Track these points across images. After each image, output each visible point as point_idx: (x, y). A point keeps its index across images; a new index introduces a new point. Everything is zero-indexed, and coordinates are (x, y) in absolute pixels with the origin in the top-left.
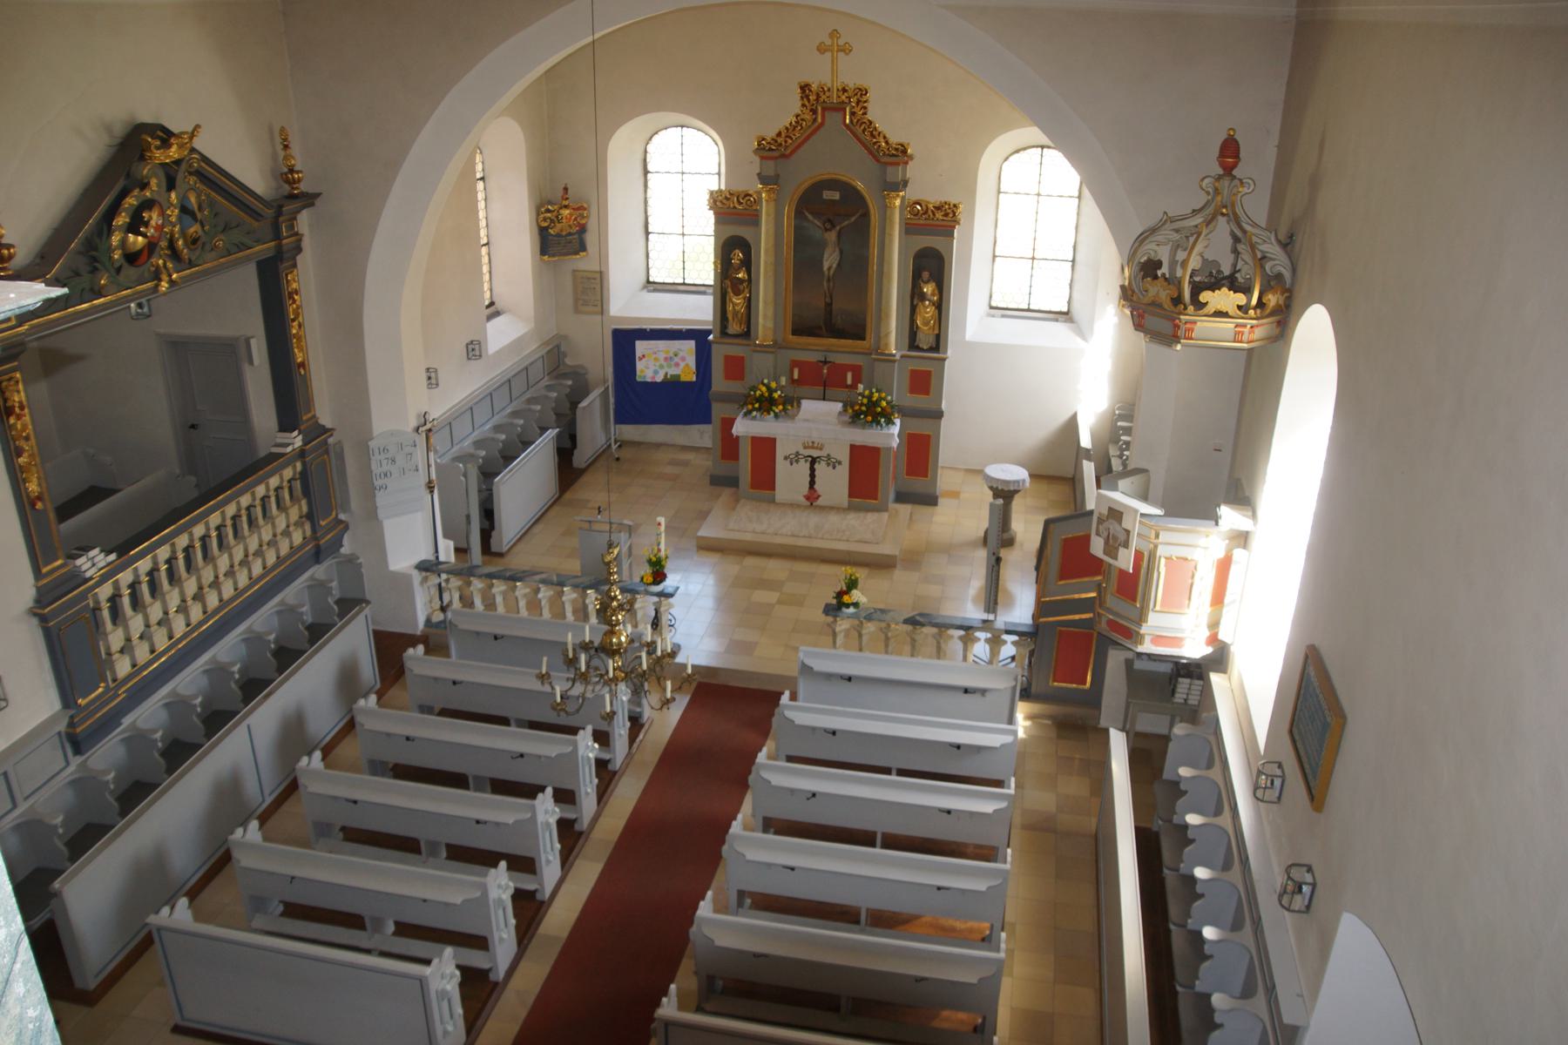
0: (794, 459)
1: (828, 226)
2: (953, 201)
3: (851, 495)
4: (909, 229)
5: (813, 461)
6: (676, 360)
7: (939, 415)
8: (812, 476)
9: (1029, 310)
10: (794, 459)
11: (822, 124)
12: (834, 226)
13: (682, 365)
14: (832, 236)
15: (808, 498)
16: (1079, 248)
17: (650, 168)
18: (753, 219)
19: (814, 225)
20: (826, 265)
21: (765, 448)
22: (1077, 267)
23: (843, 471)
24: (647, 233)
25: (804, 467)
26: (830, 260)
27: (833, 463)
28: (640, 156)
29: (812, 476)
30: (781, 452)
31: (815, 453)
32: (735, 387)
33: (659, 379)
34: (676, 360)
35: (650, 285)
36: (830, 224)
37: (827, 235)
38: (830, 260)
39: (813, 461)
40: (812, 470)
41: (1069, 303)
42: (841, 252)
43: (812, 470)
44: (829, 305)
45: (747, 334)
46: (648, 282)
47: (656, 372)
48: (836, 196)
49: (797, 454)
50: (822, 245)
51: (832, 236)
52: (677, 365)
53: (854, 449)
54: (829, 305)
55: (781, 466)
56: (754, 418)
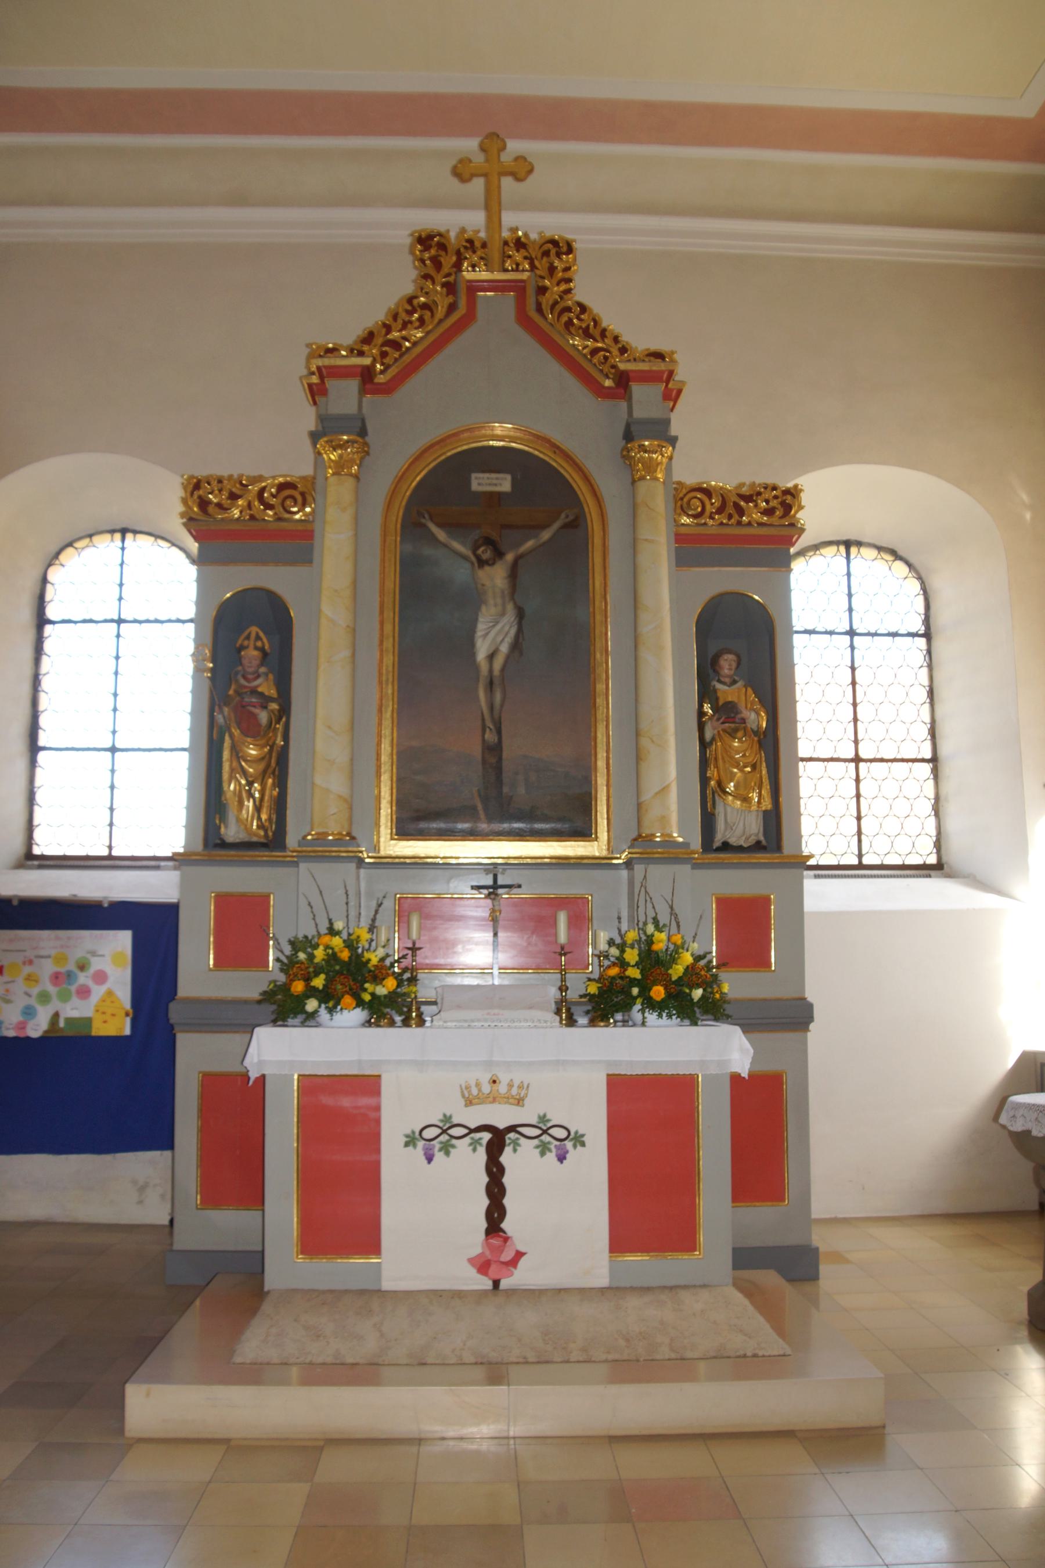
0: (436, 1139)
1: (486, 553)
3: (618, 1244)
4: (689, 550)
5: (498, 1140)
6: (83, 979)
7: (793, 1016)
8: (496, 1190)
9: (860, 868)
10: (436, 1139)
11: (470, 317)
12: (499, 554)
13: (98, 992)
14: (496, 577)
15: (483, 1266)
16: (945, 730)
17: (51, 613)
18: (299, 544)
19: (451, 554)
20: (481, 655)
22: (947, 769)
23: (593, 1162)
24: (34, 748)
25: (469, 1163)
26: (492, 635)
28: (29, 583)
29: (496, 1190)
31: (501, 1117)
33: (37, 1028)
34: (83, 979)
35: (29, 859)
36: (491, 548)
37: (483, 574)
38: (492, 635)
39: (498, 1140)
40: (495, 1171)
41: (938, 845)
42: (521, 614)
43: (495, 1171)
44: (494, 751)
45: (272, 841)
46: (29, 856)
47: (29, 1012)
48: (504, 484)
49: (447, 1126)
50: (471, 601)
51: (496, 577)
52: (84, 992)
54: (494, 751)
56: (310, 1019)
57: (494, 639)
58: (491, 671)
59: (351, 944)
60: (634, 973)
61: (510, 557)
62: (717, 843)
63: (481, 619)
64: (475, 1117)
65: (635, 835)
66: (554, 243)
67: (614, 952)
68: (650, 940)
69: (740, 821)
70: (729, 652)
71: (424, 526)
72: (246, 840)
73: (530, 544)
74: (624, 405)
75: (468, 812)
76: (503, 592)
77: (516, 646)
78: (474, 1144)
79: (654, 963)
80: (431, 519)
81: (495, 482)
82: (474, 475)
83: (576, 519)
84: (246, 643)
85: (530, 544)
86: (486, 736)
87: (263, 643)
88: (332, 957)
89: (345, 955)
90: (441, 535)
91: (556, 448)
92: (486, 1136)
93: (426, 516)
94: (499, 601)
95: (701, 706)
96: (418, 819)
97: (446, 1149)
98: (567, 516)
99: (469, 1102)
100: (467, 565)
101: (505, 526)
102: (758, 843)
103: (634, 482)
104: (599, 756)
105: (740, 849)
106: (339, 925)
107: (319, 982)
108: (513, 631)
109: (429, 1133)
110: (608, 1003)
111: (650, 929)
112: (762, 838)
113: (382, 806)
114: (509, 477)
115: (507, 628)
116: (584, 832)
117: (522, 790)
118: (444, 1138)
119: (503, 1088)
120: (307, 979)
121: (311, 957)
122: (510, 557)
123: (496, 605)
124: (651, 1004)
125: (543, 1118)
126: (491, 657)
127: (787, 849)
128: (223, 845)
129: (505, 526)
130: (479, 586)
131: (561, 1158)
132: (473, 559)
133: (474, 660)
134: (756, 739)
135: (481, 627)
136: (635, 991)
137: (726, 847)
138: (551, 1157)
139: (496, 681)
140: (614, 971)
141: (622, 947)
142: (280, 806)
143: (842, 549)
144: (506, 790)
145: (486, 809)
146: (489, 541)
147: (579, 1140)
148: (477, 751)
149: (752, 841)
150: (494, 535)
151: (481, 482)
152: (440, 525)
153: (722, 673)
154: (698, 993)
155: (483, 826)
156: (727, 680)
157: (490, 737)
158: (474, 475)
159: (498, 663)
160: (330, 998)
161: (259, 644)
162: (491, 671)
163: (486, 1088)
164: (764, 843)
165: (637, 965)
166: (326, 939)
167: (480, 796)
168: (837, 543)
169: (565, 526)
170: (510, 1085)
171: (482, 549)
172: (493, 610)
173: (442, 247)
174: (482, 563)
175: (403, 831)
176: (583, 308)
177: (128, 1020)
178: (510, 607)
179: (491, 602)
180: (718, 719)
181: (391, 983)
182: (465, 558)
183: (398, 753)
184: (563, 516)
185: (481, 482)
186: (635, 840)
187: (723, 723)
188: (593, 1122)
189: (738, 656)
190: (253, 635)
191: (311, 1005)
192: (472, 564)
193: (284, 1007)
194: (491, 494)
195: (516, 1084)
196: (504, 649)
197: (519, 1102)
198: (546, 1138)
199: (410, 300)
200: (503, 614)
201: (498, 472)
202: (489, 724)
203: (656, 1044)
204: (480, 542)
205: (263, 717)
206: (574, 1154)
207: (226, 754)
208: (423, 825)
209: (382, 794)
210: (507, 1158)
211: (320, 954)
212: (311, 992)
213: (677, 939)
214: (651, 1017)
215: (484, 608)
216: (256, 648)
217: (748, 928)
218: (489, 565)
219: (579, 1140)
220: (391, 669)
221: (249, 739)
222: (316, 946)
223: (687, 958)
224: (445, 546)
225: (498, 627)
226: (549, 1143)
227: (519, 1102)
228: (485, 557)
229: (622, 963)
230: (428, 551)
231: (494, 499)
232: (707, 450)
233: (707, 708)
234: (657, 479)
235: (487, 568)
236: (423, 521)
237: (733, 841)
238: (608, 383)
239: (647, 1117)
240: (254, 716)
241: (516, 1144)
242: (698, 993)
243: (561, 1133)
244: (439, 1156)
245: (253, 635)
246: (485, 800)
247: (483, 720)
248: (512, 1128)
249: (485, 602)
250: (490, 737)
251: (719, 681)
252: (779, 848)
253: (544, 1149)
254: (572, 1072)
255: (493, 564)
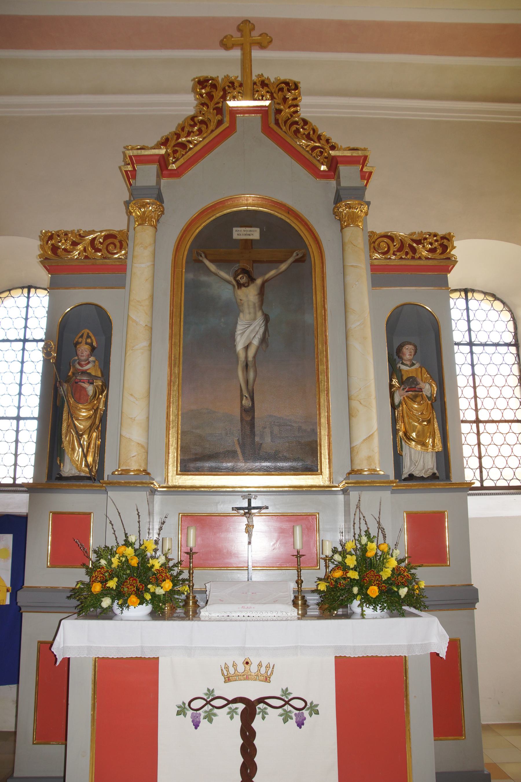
2: (441, 232)
4: (381, 275)
5: (250, 710)
7: (462, 599)
8: (248, 750)
10: (200, 710)
11: (232, 129)
12: (252, 280)
14: (250, 295)
18: (116, 273)
19: (220, 282)
20: (240, 347)
21: (129, 687)
23: (324, 728)
25: (227, 728)
26: (247, 333)
27: (297, 711)
29: (248, 750)
30: (171, 692)
31: (252, 691)
32: (72, 577)
37: (241, 293)
38: (247, 333)
39: (250, 710)
40: (248, 734)
42: (267, 319)
43: (248, 734)
44: (248, 413)
48: (255, 234)
49: (210, 699)
50: (233, 310)
51: (250, 295)
53: (349, 670)
54: (248, 413)
55: (171, 731)
57: (248, 336)
58: (246, 357)
59: (141, 553)
60: (354, 575)
61: (259, 281)
62: (405, 476)
63: (239, 323)
64: (232, 691)
65: (349, 470)
66: (287, 83)
67: (338, 557)
68: (364, 549)
69: (420, 459)
70: (410, 343)
71: (202, 262)
72: (77, 475)
73: (272, 273)
74: (333, 183)
75: (231, 455)
76: (254, 304)
77: (264, 340)
78: (232, 714)
79: (368, 565)
80: (206, 257)
81: (248, 233)
82: (234, 229)
83: (303, 257)
84: (80, 340)
85: (272, 273)
86: (243, 402)
87: (92, 340)
88: (125, 564)
89: (134, 562)
90: (212, 267)
91: (289, 211)
92: (241, 706)
93: (203, 255)
94: (252, 310)
95: (391, 381)
96: (196, 460)
97: (209, 717)
98: (298, 255)
99: (228, 679)
100: (230, 287)
101: (254, 262)
102: (434, 474)
103: (342, 228)
104: (322, 415)
105: (422, 479)
106: (132, 539)
107: (112, 584)
108: (262, 330)
109: (196, 704)
110: (334, 601)
111: (364, 540)
112: (436, 471)
113: (170, 451)
114: (258, 230)
115: (257, 328)
116: (312, 469)
117: (268, 439)
118: (208, 708)
119: (254, 668)
120: (104, 582)
121: (110, 563)
122: (259, 281)
123: (250, 313)
124: (367, 600)
125: (285, 692)
126: (247, 348)
127: (454, 479)
128: (61, 478)
129: (254, 262)
130: (239, 301)
131: (300, 724)
132: (234, 283)
133: (235, 350)
134: (429, 402)
135: (240, 328)
136: (355, 590)
137: (411, 477)
138: (292, 723)
139: (250, 364)
140: (338, 574)
141: (344, 553)
142: (101, 451)
143: (463, 294)
144: (257, 439)
145: (243, 453)
146: (244, 271)
147: (314, 710)
148: (237, 412)
149: (429, 473)
150: (248, 268)
151: (239, 233)
152: (211, 261)
153: (405, 358)
154: (403, 592)
155: (241, 465)
156: (408, 363)
157: (246, 403)
158: (234, 229)
159: (251, 352)
160: (120, 596)
161: (89, 341)
162: (246, 357)
163: (241, 668)
164: (438, 474)
165: (355, 569)
166: (122, 549)
167: (239, 443)
168: (460, 290)
169: (296, 261)
170: (260, 665)
171: (241, 276)
172: (248, 317)
173: (214, 86)
174: (240, 285)
175: (185, 469)
176: (305, 122)
177: (8, 594)
178: (259, 314)
179: (246, 311)
180: (404, 389)
181: (168, 585)
182: (229, 282)
183: (182, 414)
184: (295, 254)
185: (239, 233)
186: (349, 474)
187: (407, 392)
188: (323, 692)
189: (415, 347)
190: (85, 336)
191: (106, 602)
192: (234, 286)
193: (86, 605)
194: (246, 241)
195: (264, 665)
196: (256, 342)
197: (267, 679)
198: (287, 708)
199: (193, 118)
200: (255, 319)
201: (251, 227)
202: (245, 393)
203: (371, 632)
204: (239, 271)
205: (90, 389)
206: (310, 721)
207: (65, 415)
208: (199, 464)
209: (171, 442)
210: (257, 724)
211: (115, 561)
212: (106, 592)
213: (384, 547)
214: (369, 611)
215: (241, 315)
216: (87, 343)
217: (429, 536)
218: (246, 287)
219: (314, 710)
220: (177, 356)
221: (80, 406)
222: (113, 555)
223: (393, 563)
224: (216, 274)
225: (251, 328)
226: (290, 711)
227: (267, 679)
228: (242, 281)
229: (343, 566)
230: (204, 278)
231: (248, 244)
232: (391, 211)
233: (395, 382)
234: (358, 226)
235: (243, 289)
236: (201, 258)
237: (417, 473)
238: (323, 168)
239: (367, 691)
240: (85, 389)
241: (264, 713)
242: (403, 592)
243: (300, 704)
244: (204, 723)
245: (85, 336)
246: (242, 446)
247: (241, 390)
248: (261, 700)
249: (243, 312)
250: (246, 403)
251: (402, 363)
252: (448, 477)
253: (286, 718)
254: (307, 654)
255: (248, 286)
